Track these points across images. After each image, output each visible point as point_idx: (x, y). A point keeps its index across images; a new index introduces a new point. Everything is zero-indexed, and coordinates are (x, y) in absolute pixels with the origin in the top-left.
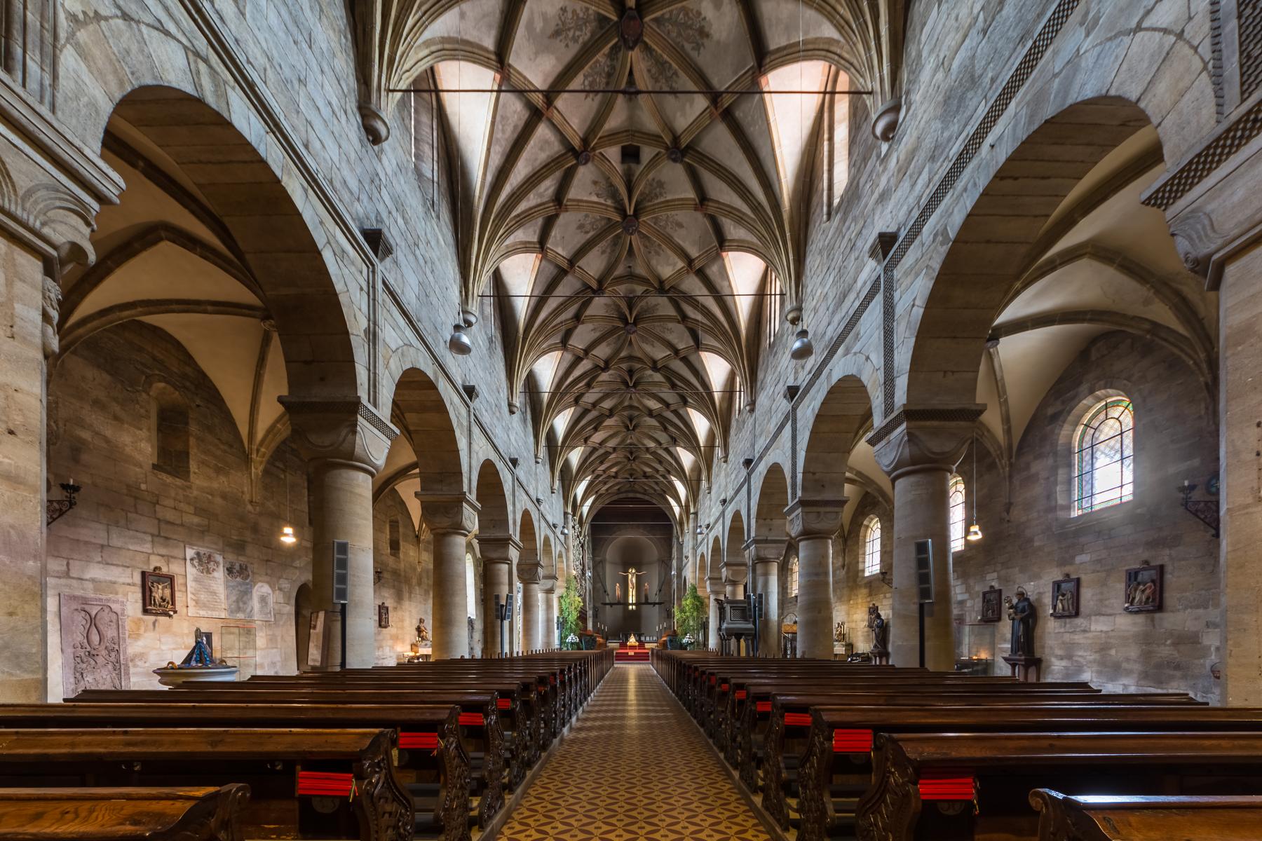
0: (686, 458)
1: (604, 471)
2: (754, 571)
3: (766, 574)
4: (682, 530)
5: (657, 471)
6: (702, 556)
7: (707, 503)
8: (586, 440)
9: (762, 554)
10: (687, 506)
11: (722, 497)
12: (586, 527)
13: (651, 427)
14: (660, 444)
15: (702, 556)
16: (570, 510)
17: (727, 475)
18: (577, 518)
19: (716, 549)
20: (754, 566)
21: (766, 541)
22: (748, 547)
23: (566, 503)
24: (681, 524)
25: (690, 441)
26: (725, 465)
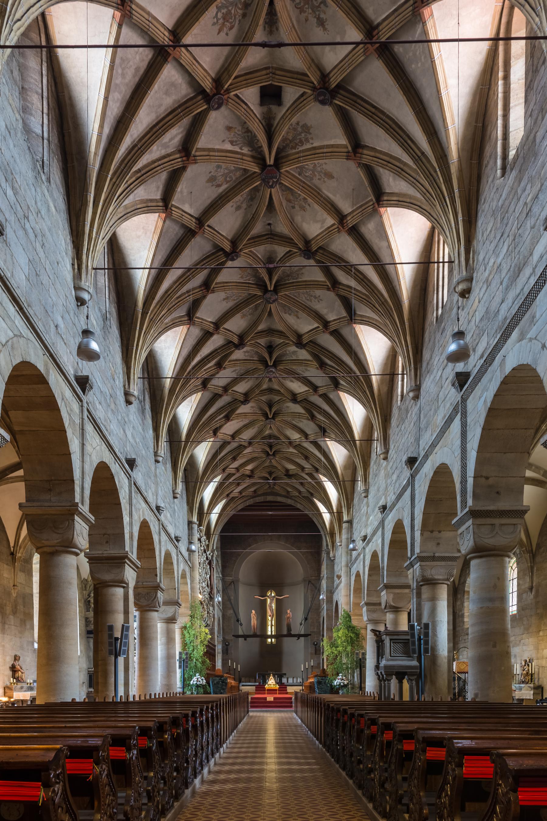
1: (237, 469)
2: (419, 595)
3: (434, 599)
4: (333, 543)
5: (303, 469)
7: (364, 509)
8: (215, 432)
11: (382, 503)
14: (306, 436)
16: (195, 519)
17: (387, 476)
18: (204, 528)
20: (419, 588)
22: (411, 565)
24: (332, 534)
26: (384, 463)
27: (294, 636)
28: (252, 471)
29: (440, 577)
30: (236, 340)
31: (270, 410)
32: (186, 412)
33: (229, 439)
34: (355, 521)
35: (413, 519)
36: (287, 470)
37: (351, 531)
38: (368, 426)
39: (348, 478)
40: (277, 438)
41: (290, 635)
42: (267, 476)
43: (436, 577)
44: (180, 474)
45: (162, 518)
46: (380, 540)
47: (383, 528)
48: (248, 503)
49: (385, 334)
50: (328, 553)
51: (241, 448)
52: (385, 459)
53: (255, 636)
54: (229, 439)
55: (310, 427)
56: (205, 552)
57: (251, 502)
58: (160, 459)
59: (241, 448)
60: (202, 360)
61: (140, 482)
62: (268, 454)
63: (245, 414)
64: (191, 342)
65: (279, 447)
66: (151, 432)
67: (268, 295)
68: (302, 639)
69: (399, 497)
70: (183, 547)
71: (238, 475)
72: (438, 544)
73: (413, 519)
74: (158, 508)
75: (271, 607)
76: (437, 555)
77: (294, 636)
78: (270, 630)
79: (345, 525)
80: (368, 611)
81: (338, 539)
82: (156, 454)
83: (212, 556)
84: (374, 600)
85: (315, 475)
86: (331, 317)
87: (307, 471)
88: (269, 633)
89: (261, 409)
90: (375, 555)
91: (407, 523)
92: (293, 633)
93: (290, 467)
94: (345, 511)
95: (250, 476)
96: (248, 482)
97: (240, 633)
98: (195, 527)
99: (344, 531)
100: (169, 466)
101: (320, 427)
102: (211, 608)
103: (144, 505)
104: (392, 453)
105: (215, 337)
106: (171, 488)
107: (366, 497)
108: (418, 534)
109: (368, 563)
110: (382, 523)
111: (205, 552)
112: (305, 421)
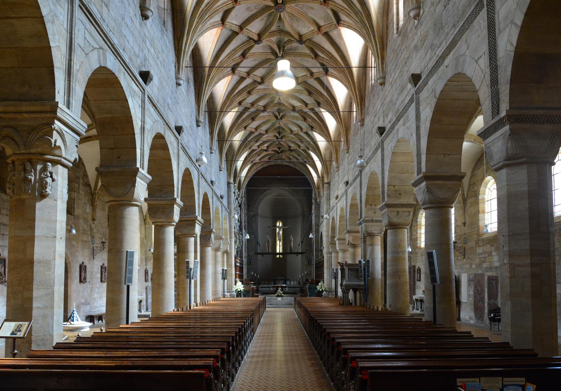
0: (321, 142)
1: (259, 147)
2: (365, 242)
3: (372, 245)
4: (319, 192)
5: (299, 146)
6: (333, 219)
8: (245, 128)
9: (369, 230)
10: (323, 177)
11: (345, 179)
12: (243, 190)
13: (294, 117)
14: (301, 129)
15: (333, 219)
16: (232, 181)
18: (236, 185)
20: (365, 238)
21: (372, 221)
22: (360, 224)
23: (229, 175)
24: (318, 188)
25: (323, 131)
26: (347, 155)
27: (295, 253)
28: (268, 147)
29: (376, 232)
30: (259, 80)
31: (279, 115)
32: (229, 119)
33: (254, 130)
34: (332, 184)
35: (361, 197)
36: (290, 147)
37: (330, 190)
38: (338, 130)
39: (327, 158)
40: (283, 129)
42: (277, 150)
43: (374, 232)
44: (224, 156)
45: (214, 188)
46: (345, 202)
47: (347, 195)
48: (264, 166)
49: (346, 86)
50: (316, 200)
51: (261, 135)
52: (348, 152)
53: (268, 253)
54: (254, 130)
55: (304, 125)
56: (237, 199)
57: (267, 165)
58: (213, 151)
59: (261, 135)
60: (239, 91)
61: (203, 173)
62: (278, 138)
63: (264, 117)
64: (234, 82)
65: (284, 134)
66: (208, 136)
68: (300, 255)
69: (355, 180)
70: (225, 201)
71: (259, 150)
72: (375, 212)
73: (361, 197)
74: (212, 182)
75: (279, 233)
76: (374, 219)
77: (295, 253)
78: (279, 248)
79: (325, 185)
80: (339, 243)
81: (322, 193)
82: (211, 148)
83: (242, 201)
84: (342, 237)
85: (307, 151)
86: (314, 70)
87: (302, 148)
88: (278, 251)
89: (274, 114)
90: (342, 209)
93: (292, 145)
94: (325, 176)
95: (266, 151)
97: (259, 251)
98: (232, 186)
99: (325, 189)
100: (217, 152)
101: (310, 125)
102: (241, 236)
103: (205, 183)
105: (247, 79)
106: (218, 165)
107: (338, 171)
108: (363, 206)
109: (339, 213)
110: (346, 191)
111: (237, 199)
112: (301, 121)
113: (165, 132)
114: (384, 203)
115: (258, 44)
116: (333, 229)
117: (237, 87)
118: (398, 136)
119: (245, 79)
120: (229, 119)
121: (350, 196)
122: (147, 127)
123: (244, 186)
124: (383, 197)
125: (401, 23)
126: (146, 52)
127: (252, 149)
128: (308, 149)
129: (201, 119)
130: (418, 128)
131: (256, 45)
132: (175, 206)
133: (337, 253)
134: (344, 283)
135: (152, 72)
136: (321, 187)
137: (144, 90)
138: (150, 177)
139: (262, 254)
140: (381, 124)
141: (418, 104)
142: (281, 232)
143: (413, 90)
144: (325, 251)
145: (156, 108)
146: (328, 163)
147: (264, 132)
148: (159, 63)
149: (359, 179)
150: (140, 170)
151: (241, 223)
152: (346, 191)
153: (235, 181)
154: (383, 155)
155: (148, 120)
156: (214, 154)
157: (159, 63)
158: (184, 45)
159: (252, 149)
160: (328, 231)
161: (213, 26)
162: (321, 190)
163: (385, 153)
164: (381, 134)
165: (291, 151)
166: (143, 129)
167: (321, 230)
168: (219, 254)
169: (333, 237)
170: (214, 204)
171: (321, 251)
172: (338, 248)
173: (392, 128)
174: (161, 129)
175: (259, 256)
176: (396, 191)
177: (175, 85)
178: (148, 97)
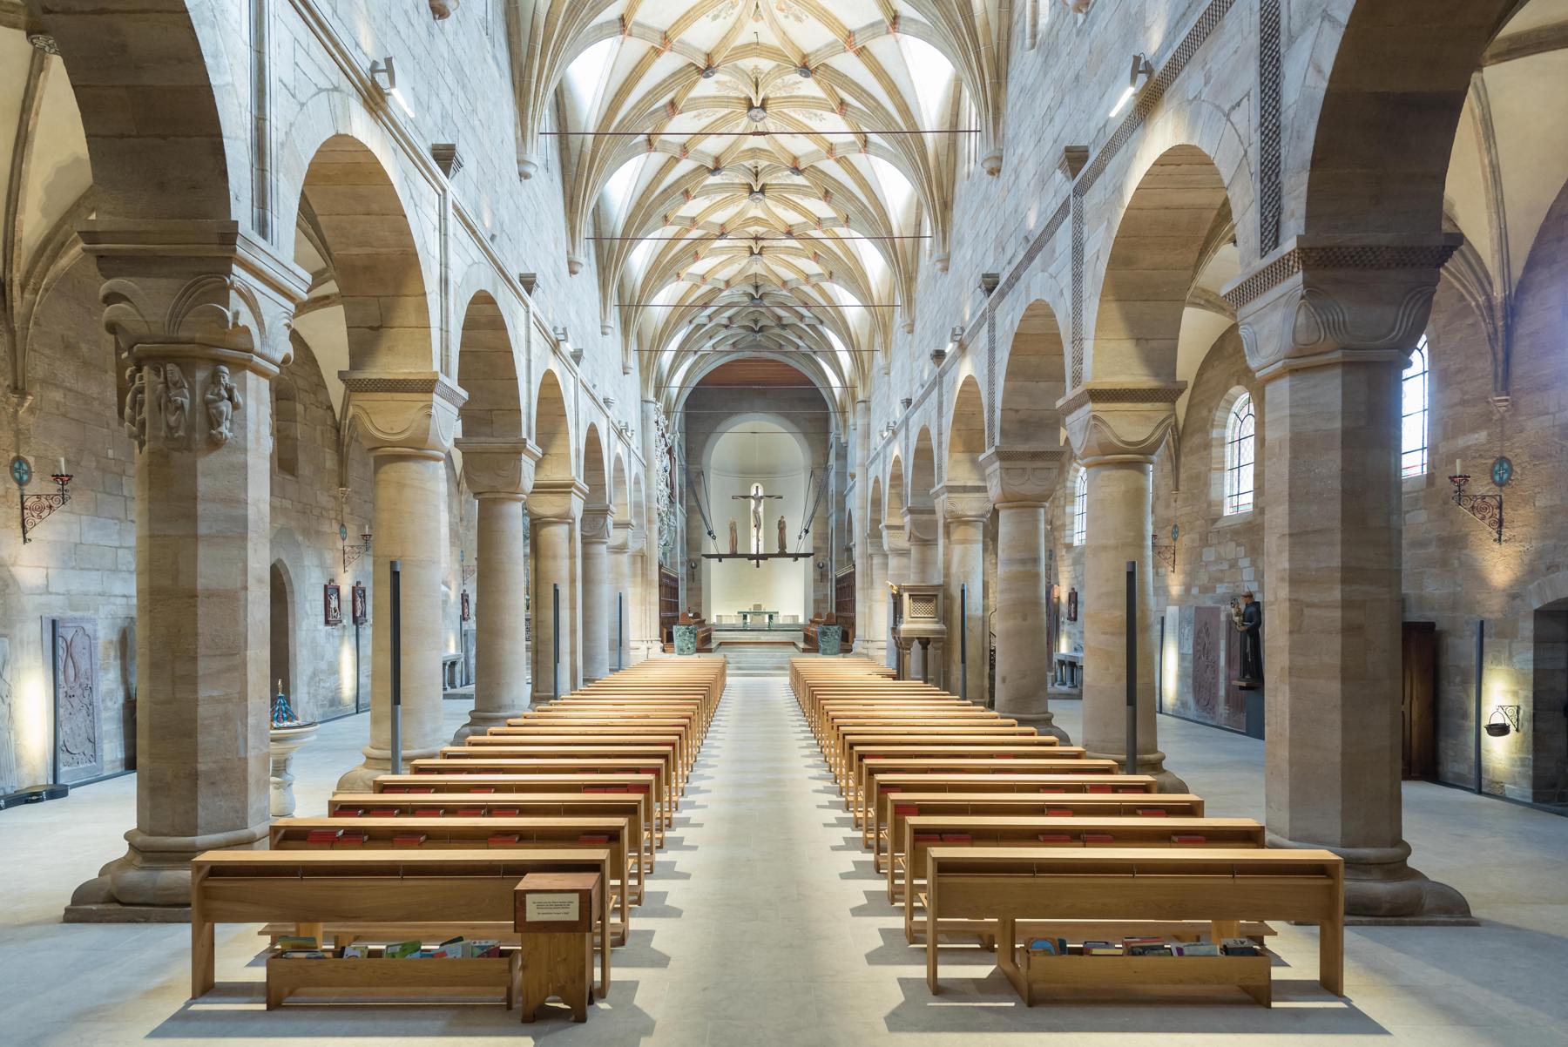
1: (710, 318)
4: (845, 421)
5: (802, 317)
10: (853, 387)
12: (677, 417)
15: (877, 481)
16: (651, 397)
19: (897, 478)
23: (645, 382)
24: (843, 412)
28: (730, 318)
35: (940, 434)
36: (780, 318)
41: (782, 554)
63: (722, 250)
67: (753, 112)
68: (801, 560)
70: (635, 443)
73: (940, 434)
74: (606, 401)
75: (756, 512)
79: (860, 406)
81: (851, 421)
85: (820, 327)
87: (807, 321)
91: (934, 433)
92: (788, 551)
94: (858, 384)
95: (726, 327)
96: (723, 333)
97: (713, 552)
99: (859, 414)
104: (918, 326)
107: (888, 374)
110: (906, 420)
113: (496, 291)
114: (993, 450)
115: (708, 76)
116: (876, 503)
117: (660, 182)
118: (1028, 295)
119: (678, 160)
120: (640, 258)
121: (914, 432)
122: (455, 277)
123: (680, 407)
124: (992, 437)
125: (1044, 20)
126: (445, 96)
127: (696, 322)
128: (822, 322)
129: (580, 257)
130: (1077, 278)
131: (703, 82)
132: (524, 457)
133: (886, 556)
134: (903, 627)
135: (462, 150)
136: (849, 408)
137: (444, 190)
138: (464, 394)
139: (720, 557)
140: (989, 268)
141: (1079, 219)
142: (761, 509)
143: (1068, 187)
144: (857, 552)
145: (474, 232)
146: (865, 355)
147: (722, 286)
148: (477, 123)
149: (935, 393)
150: (442, 377)
151: (672, 488)
152: (906, 420)
153: (657, 395)
154: (992, 340)
155: (454, 259)
156: (609, 337)
157: (477, 123)
158: (534, 80)
159: (696, 322)
160: (864, 508)
161: (601, 33)
162: (850, 416)
163: (998, 334)
164: (990, 291)
165: (784, 327)
166: (444, 282)
167: (848, 506)
168: (625, 559)
169: (876, 522)
170: (612, 449)
171: (849, 550)
172: (886, 547)
173: (1015, 277)
174: (485, 280)
175: (714, 561)
176: (1021, 422)
177: (516, 176)
178: (455, 206)
